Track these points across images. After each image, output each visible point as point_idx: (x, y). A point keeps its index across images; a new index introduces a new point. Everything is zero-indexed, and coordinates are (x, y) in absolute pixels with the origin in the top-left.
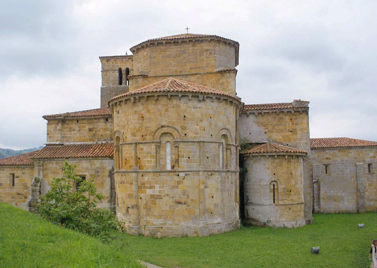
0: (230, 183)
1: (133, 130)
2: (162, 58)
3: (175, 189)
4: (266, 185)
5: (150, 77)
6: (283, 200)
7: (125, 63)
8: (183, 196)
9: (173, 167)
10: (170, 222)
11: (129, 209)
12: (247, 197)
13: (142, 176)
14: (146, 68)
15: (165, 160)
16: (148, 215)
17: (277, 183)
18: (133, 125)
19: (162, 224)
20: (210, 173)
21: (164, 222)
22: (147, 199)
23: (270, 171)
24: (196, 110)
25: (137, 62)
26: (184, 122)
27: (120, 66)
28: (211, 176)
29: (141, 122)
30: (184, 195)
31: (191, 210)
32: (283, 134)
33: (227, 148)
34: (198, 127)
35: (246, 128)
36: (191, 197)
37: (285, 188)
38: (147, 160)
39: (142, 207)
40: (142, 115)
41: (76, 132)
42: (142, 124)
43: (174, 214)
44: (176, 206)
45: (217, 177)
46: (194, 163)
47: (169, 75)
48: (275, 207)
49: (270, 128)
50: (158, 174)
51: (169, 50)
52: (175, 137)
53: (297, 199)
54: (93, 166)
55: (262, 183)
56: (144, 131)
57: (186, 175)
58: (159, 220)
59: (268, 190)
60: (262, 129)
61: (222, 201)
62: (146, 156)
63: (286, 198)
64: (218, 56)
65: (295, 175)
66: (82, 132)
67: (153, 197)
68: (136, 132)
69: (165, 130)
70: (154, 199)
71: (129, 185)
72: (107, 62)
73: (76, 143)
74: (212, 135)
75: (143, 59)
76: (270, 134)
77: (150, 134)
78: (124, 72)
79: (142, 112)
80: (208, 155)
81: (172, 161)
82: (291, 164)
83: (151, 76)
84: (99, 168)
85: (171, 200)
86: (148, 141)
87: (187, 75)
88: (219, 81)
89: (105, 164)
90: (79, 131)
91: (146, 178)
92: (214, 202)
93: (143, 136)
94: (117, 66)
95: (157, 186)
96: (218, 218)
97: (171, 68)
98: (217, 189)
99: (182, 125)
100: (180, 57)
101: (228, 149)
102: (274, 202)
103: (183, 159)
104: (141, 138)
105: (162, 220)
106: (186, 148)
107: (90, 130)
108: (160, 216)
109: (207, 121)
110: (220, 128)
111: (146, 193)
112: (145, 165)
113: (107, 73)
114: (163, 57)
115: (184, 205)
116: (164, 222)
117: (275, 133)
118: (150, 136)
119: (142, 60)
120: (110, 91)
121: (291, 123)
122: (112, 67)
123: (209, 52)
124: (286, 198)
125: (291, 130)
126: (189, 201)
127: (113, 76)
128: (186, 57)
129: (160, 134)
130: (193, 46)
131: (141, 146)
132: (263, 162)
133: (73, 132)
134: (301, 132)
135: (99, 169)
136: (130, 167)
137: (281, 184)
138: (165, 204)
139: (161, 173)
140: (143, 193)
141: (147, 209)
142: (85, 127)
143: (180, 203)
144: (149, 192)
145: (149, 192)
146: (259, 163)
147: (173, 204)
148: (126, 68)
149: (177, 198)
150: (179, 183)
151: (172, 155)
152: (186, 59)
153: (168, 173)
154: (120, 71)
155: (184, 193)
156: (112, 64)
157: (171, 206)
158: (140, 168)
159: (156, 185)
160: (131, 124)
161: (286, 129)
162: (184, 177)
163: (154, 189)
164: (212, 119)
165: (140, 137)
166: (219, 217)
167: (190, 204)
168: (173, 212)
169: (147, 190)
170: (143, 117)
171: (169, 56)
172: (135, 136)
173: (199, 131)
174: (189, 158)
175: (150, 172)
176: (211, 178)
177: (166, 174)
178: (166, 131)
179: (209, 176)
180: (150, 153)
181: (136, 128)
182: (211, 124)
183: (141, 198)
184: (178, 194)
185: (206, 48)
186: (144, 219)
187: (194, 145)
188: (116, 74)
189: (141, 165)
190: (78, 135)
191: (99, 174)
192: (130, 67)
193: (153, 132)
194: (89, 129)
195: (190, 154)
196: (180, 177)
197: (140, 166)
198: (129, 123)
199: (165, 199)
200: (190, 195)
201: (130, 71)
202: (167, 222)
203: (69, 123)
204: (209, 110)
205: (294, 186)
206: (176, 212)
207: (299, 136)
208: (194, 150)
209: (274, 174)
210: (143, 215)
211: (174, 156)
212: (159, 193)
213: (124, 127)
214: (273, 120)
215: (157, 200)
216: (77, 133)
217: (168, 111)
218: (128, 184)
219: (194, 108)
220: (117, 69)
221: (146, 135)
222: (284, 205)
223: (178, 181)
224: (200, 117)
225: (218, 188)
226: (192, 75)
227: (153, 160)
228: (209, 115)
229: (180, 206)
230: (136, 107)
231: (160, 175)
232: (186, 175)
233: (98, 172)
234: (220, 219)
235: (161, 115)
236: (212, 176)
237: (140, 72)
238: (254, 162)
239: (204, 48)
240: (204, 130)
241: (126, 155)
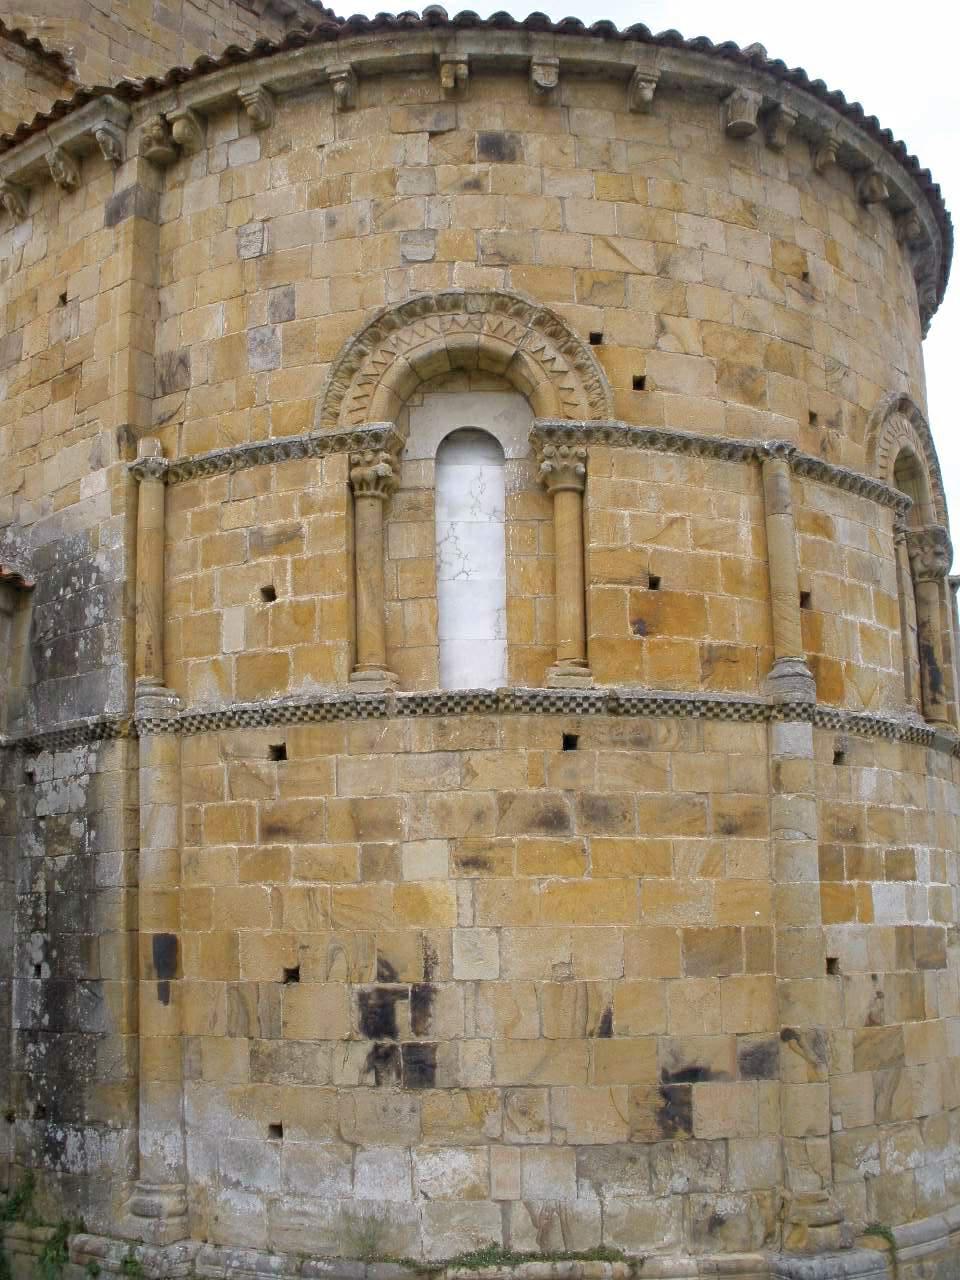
1: (731, 344)
11: (698, 1088)
13: (839, 757)
18: (735, 299)
22: (880, 973)
38: (863, 624)
39: (846, 1052)
42: (805, 321)
62: (852, 586)
70: (914, 971)
71: (713, 839)
111: (867, 916)
112: (848, 664)
131: (819, 497)
141: (883, 1065)
144: (889, 902)
145: (889, 902)
160: (704, 282)
169: (875, 884)
170: (805, 276)
172: (754, 397)
181: (764, 338)
183: (831, 963)
186: (862, 1169)
189: (820, 654)
213: (600, 286)
215: (928, 974)
218: (692, 826)
241: (655, 539)
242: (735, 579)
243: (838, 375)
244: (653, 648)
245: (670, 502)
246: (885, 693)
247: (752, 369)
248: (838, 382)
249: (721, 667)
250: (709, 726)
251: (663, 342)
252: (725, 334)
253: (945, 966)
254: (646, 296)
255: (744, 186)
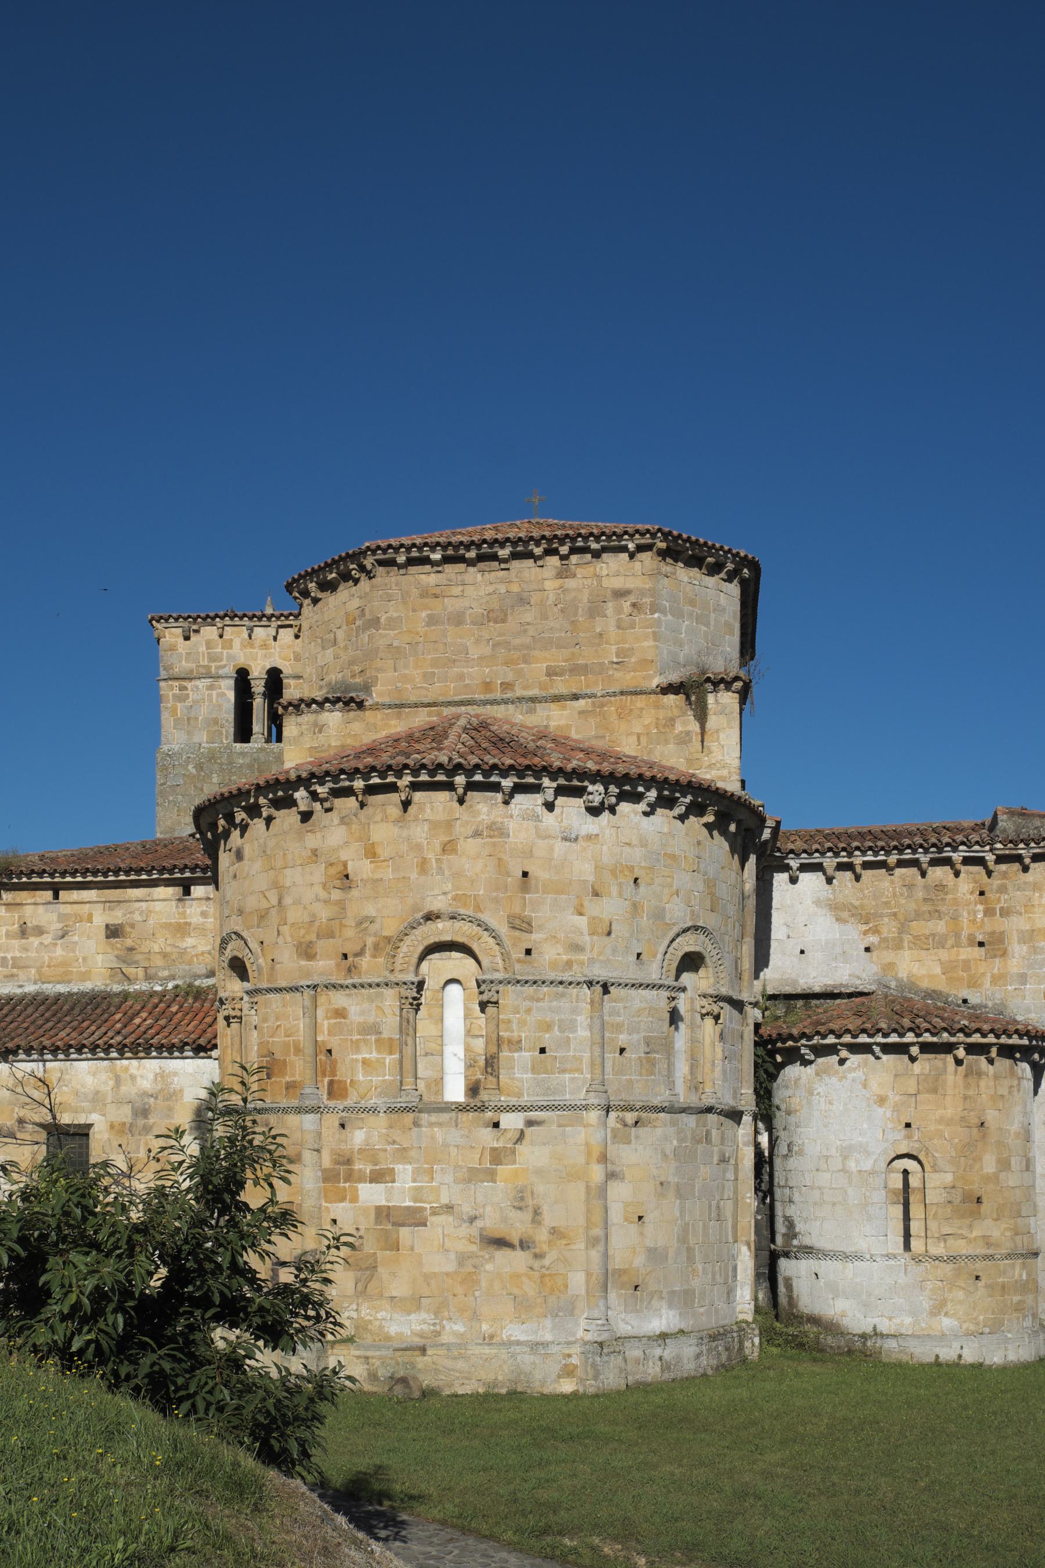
0: (716, 1160)
1: (302, 932)
2: (428, 624)
3: (483, 1181)
4: (872, 1173)
5: (376, 707)
6: (944, 1237)
7: (264, 646)
8: (513, 1214)
9: (473, 1090)
10: (459, 1328)
12: (790, 1224)
14: (357, 669)
15: (438, 1058)
16: (362, 1292)
17: (920, 1162)
18: (305, 908)
19: (421, 1335)
20: (630, 1117)
21: (434, 1324)
23: (889, 1114)
24: (573, 845)
25: (319, 640)
26: (524, 898)
27: (242, 661)
28: (633, 1129)
29: (336, 895)
30: (520, 1209)
31: (550, 1275)
32: (944, 955)
33: (704, 1011)
34: (582, 922)
35: (784, 929)
36: (549, 1219)
37: (953, 1187)
38: (364, 1058)
40: (342, 868)
41: (47, 939)
42: (341, 904)
43: (477, 1293)
44: (487, 1256)
45: (659, 1131)
46: (563, 1071)
47: (457, 698)
48: (909, 1268)
49: (889, 928)
50: (409, 1117)
51: (457, 590)
52: (485, 962)
53: (1008, 1234)
54: (123, 1089)
55: (852, 1165)
56: (350, 933)
57: (530, 1123)
58: (413, 1317)
59: (879, 1196)
60: (854, 934)
61: (683, 1239)
62: (357, 1040)
63: (960, 1228)
64: (670, 617)
65: (1000, 1129)
66: (76, 938)
67: (388, 1216)
68: (318, 937)
69: (442, 930)
70: (390, 1227)
72: (187, 638)
73: (50, 986)
74: (639, 955)
75: (344, 627)
76: (888, 956)
77: (376, 947)
78: (258, 687)
79: (343, 858)
80: (623, 1039)
81: (470, 1065)
82: (983, 1083)
83: (377, 704)
84: (152, 1096)
85: (465, 1230)
86: (365, 980)
87: (533, 700)
88: (673, 725)
89: (176, 1079)
90: (63, 937)
91: (358, 1137)
92: (649, 1243)
93: (345, 956)
94: (230, 657)
95: (404, 1172)
96: (664, 1311)
97: (465, 671)
98: (662, 1184)
99: (517, 910)
100: (504, 621)
101: (708, 1014)
102: (907, 1246)
103: (516, 1055)
104: (338, 965)
105: (423, 1315)
106: (529, 1011)
107: (113, 932)
108: (413, 1303)
109: (620, 895)
110: (674, 924)
111: (355, 1199)
112: (352, 1080)
113: (186, 688)
114: (432, 620)
115: (519, 1253)
116: (434, 1324)
117: (910, 948)
118: (374, 956)
119: (341, 635)
120: (199, 767)
121: (980, 907)
122: (206, 663)
123: (628, 603)
124: (960, 1232)
125: (980, 938)
126: (542, 1236)
127: (211, 700)
128: (528, 624)
129: (421, 948)
130: (560, 575)
131: (339, 999)
132: (859, 1074)
133: (34, 941)
134: (1025, 948)
135: (152, 1100)
136: (287, 1088)
137: (935, 1169)
138: (438, 1247)
139: (424, 1116)
140: (343, 1199)
141: (361, 1269)
142: (90, 920)
143: (501, 1243)
144: (371, 1194)
145: (371, 1194)
146: (841, 1079)
147: (474, 1248)
148: (268, 667)
149: (491, 1222)
150: (497, 1156)
151: (470, 1039)
152: (531, 633)
153: (453, 1114)
154: (242, 678)
155: (521, 1200)
156: (208, 648)
157: (462, 1259)
158: (331, 1094)
159: (401, 1166)
160: (294, 903)
161: (958, 936)
162: (522, 1132)
163: (393, 1181)
164: (642, 888)
165: (332, 962)
166: (670, 1306)
167: (545, 1248)
168: (470, 1280)
169: (360, 1186)
170: (347, 876)
171: (458, 619)
173: (587, 938)
174: (543, 1051)
175: (374, 1110)
176: (637, 1137)
177: (445, 1117)
178: (447, 938)
179: (627, 1128)
180: (374, 1029)
181: (317, 924)
182: (635, 907)
184: (493, 1205)
185: (618, 583)
187: (563, 995)
188: (223, 694)
190: (59, 952)
191: (151, 1121)
192: (287, 663)
193: (388, 939)
194: (107, 926)
195: (547, 1036)
196: (505, 1130)
197: (331, 1083)
198: (288, 901)
199: (440, 1225)
200: (545, 1209)
201: (285, 681)
202: (447, 1328)
203: (18, 901)
204: (627, 849)
205: (995, 1178)
206: (483, 1284)
207: (1014, 965)
208: (563, 1017)
209: (908, 1125)
210: (345, 1296)
211: (479, 1045)
212: (415, 1200)
213: (263, 916)
214: (902, 895)
215: (404, 1232)
216: (56, 944)
217: (454, 851)
219: (565, 839)
220: (230, 670)
221: (360, 954)
222: (952, 1259)
223: (494, 1150)
224: (591, 878)
225: (663, 1179)
226: (557, 699)
227: (390, 1059)
228: (631, 869)
229: (502, 1255)
230: (318, 835)
231: (416, 1124)
232: (530, 1123)
233: (144, 1112)
234: (672, 1313)
235: (423, 866)
236: (641, 1131)
237: (332, 688)
238: (817, 1074)
239: (606, 583)
240: (609, 934)
241: (272, 1036)
242: (298, 1050)
243: (364, 926)
244: (272, 1084)
245: (277, 1019)
246: (379, 1090)
247: (311, 942)
248: (366, 929)
249: (291, 1090)
250: (286, 1117)
251: (280, 940)
252: (299, 928)
253: (426, 1225)
254: (274, 917)
255: (312, 841)
